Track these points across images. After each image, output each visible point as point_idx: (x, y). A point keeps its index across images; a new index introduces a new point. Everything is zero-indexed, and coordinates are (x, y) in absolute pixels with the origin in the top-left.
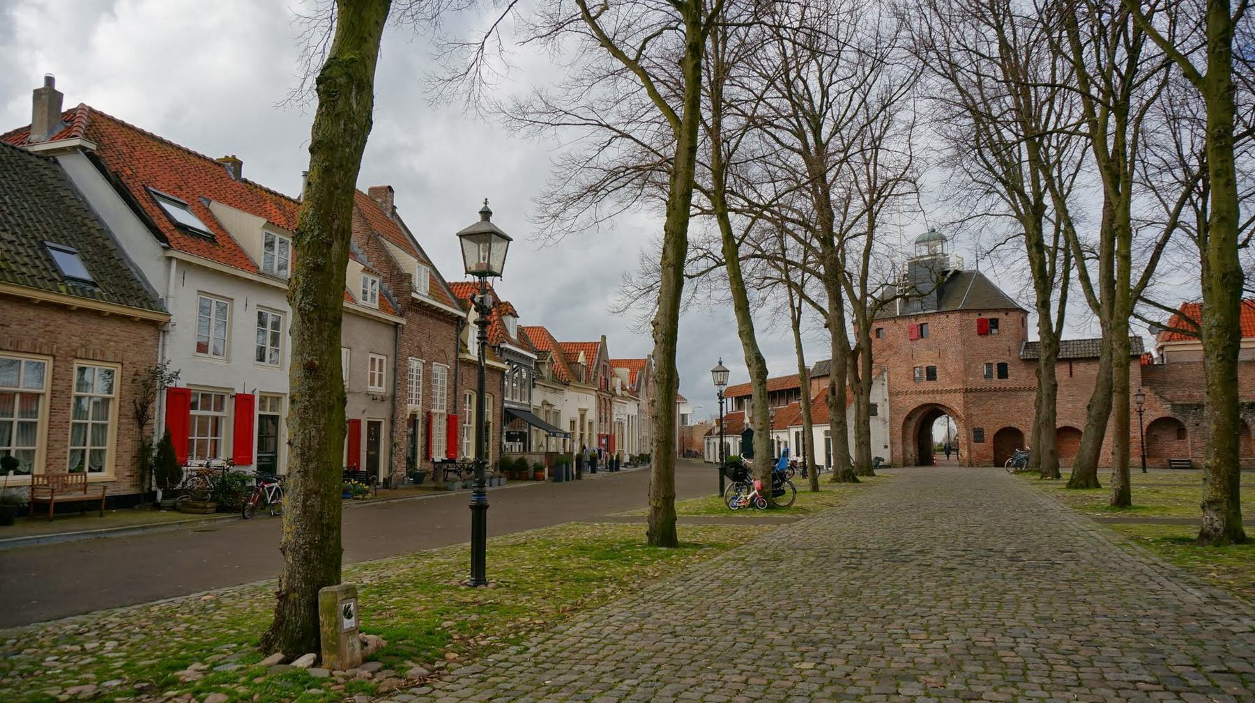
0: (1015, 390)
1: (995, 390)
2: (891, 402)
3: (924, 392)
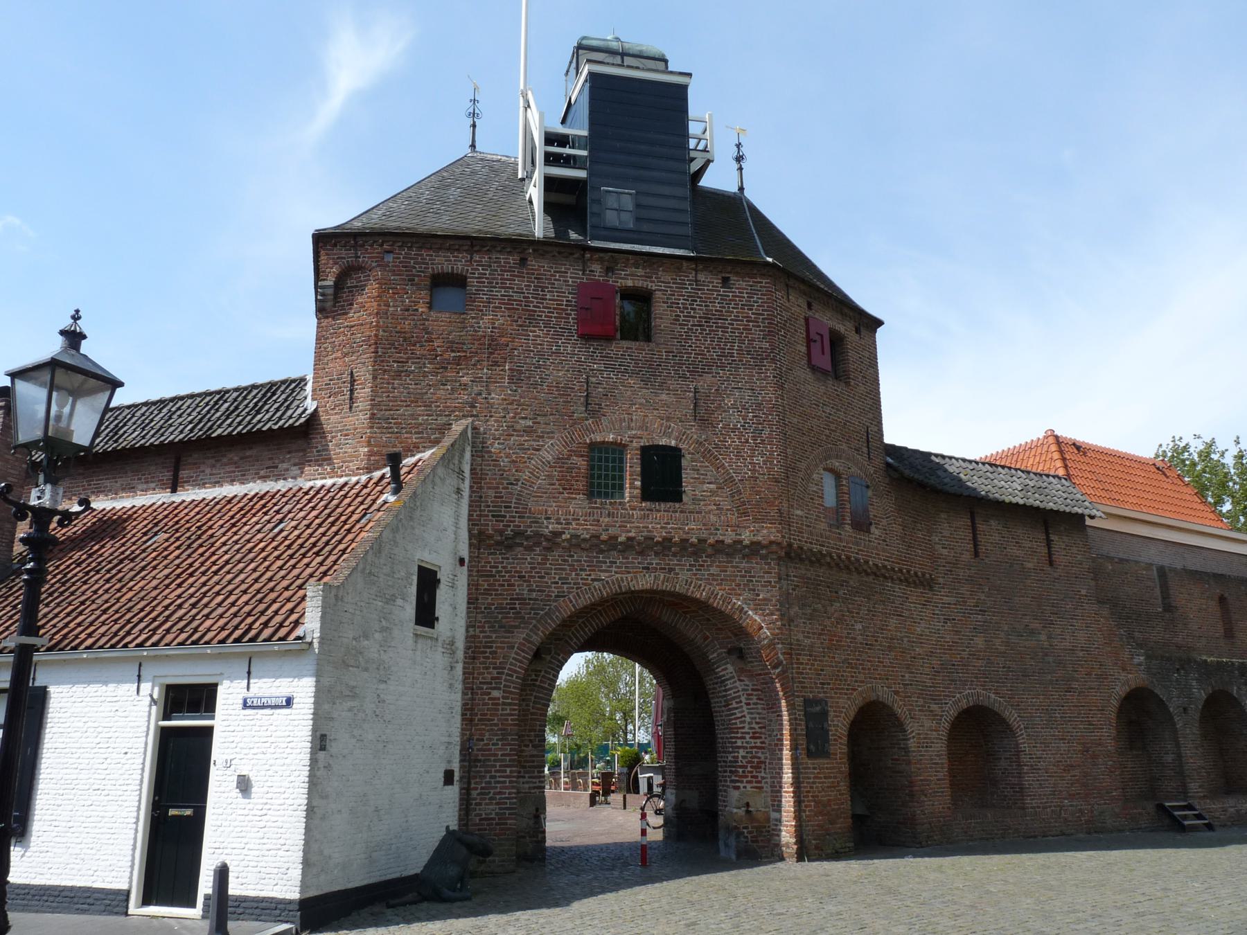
0: (880, 573)
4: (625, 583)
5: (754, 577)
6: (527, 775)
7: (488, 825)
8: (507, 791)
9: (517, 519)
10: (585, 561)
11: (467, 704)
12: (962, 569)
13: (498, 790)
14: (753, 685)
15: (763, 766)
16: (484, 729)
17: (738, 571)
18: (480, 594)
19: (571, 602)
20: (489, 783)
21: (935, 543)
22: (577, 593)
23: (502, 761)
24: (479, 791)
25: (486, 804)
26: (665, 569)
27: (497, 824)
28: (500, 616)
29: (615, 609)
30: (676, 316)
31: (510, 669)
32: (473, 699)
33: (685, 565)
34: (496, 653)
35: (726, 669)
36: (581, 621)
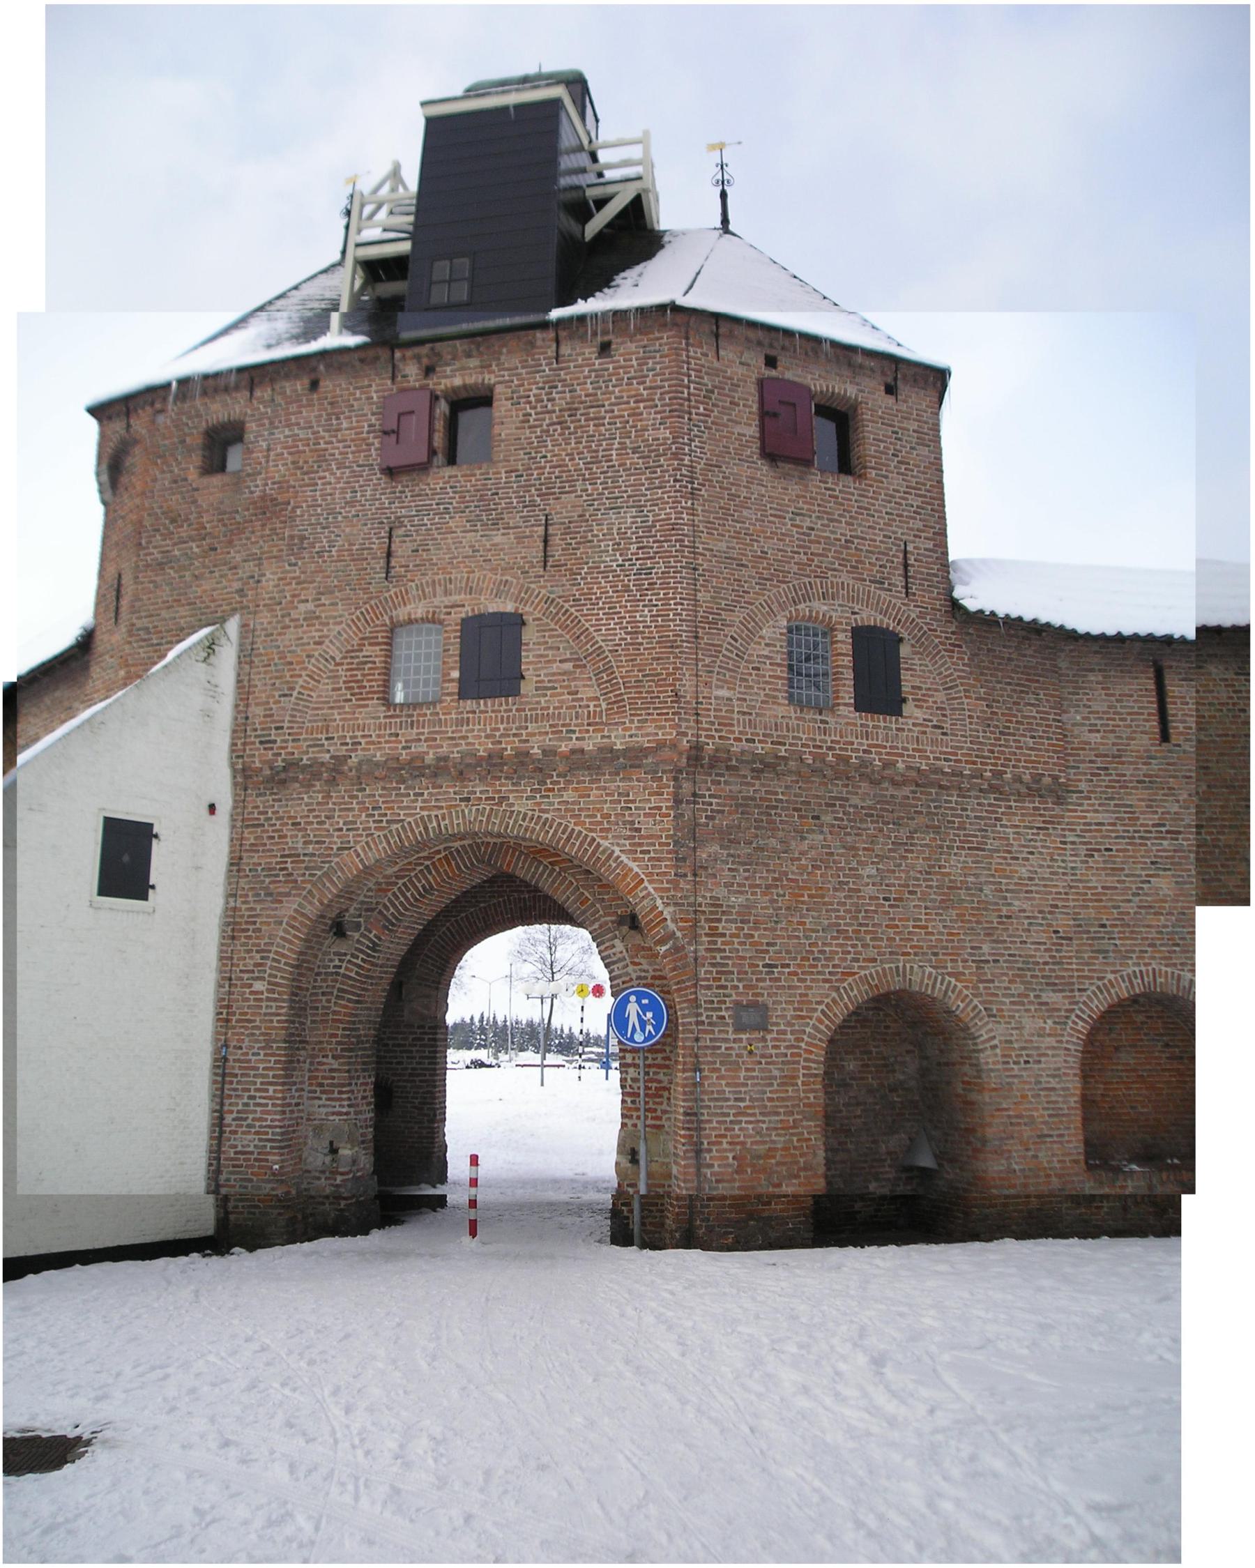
0: (922, 780)
1: (843, 771)
2: (242, 821)
3: (439, 769)
4: (435, 824)
5: (633, 801)
6: (324, 1096)
7: (244, 1160)
8: (269, 1117)
9: (290, 744)
10: (380, 796)
11: (224, 999)
12: (1131, 763)
13: (258, 1115)
14: (654, 970)
15: (666, 1094)
16: (243, 1034)
17: (607, 795)
18: (247, 851)
19: (358, 855)
20: (246, 1105)
21: (1073, 725)
22: (367, 843)
23: (263, 1076)
24: (235, 1115)
25: (243, 1133)
26: (493, 799)
27: (256, 1160)
28: (267, 880)
29: (449, 864)
30: (524, 415)
31: (277, 953)
32: (230, 993)
33: (522, 791)
34: (259, 930)
35: (614, 946)
36: (401, 882)
